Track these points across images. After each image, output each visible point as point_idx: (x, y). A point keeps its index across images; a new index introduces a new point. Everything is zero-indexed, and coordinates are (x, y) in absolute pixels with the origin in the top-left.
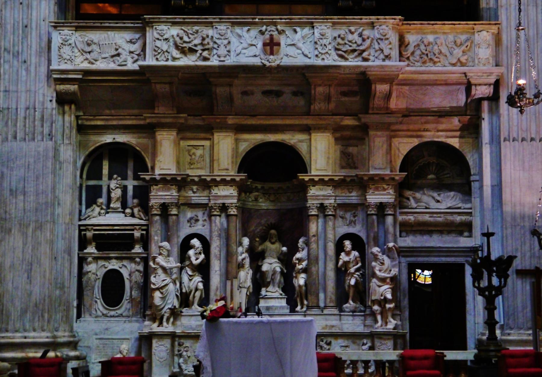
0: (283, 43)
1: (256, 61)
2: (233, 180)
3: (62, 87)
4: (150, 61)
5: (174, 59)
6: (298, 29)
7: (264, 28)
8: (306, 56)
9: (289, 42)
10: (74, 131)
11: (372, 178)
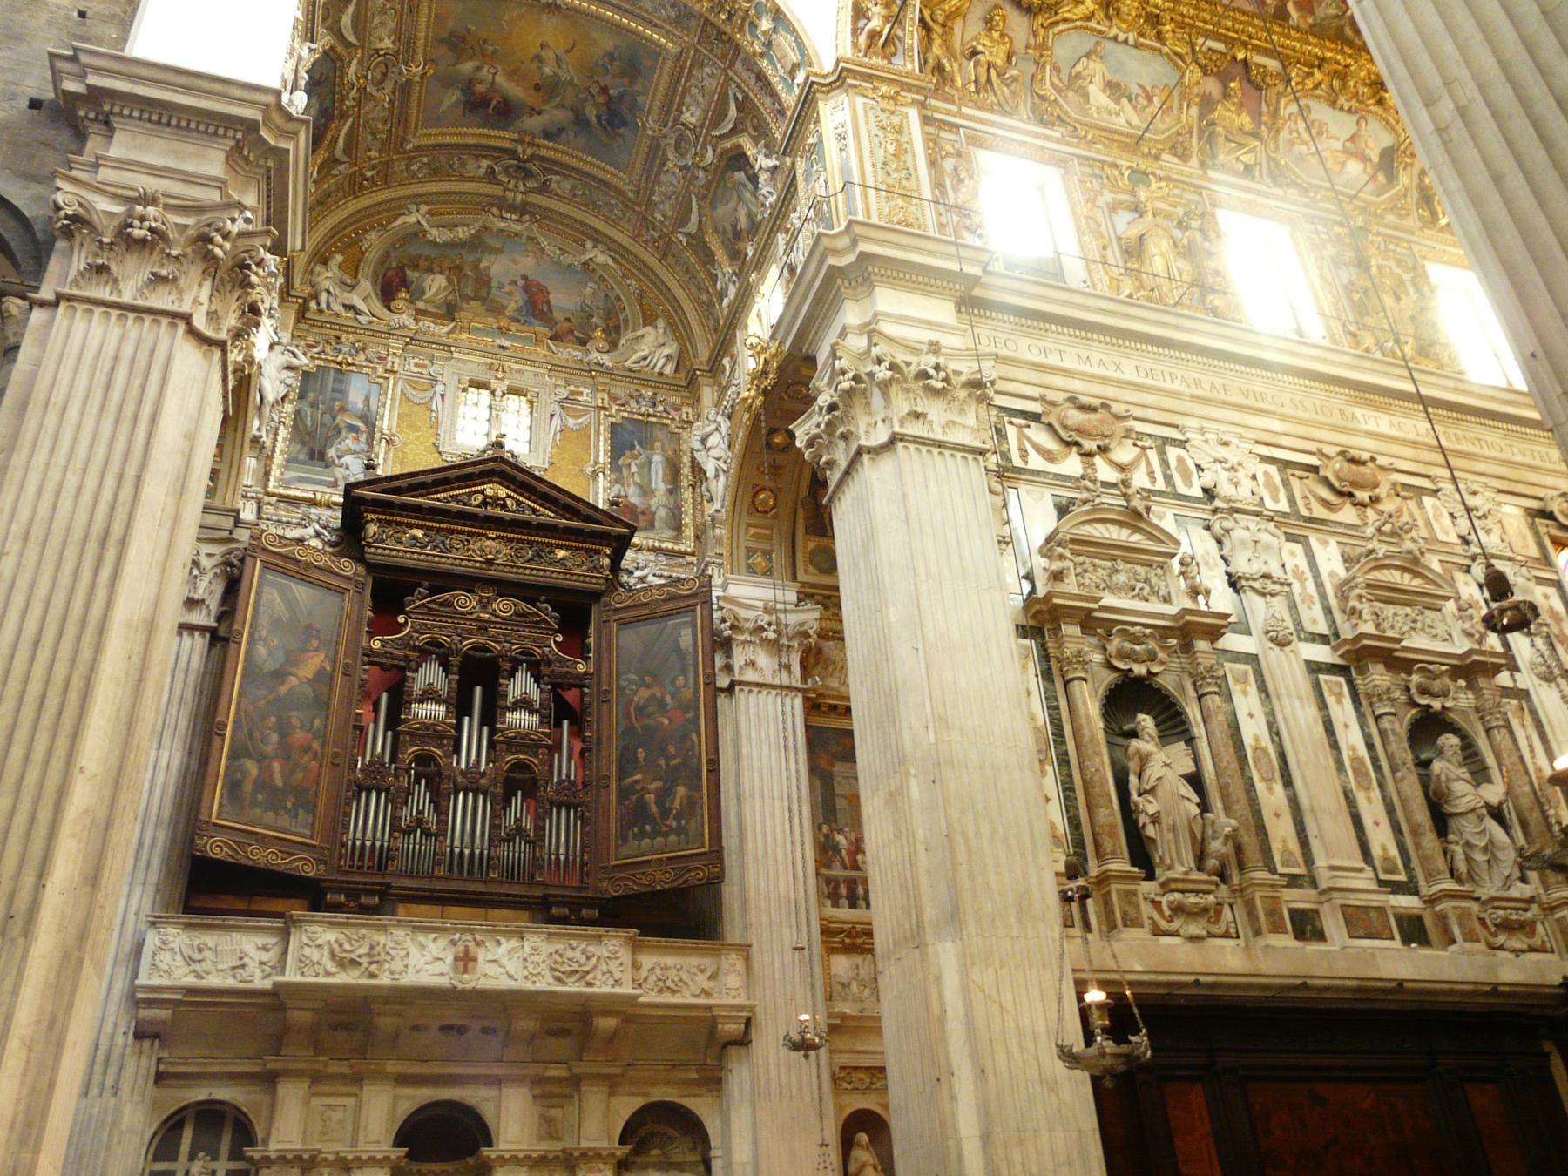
0: (481, 958)
1: (444, 982)
2: (386, 1158)
3: (144, 1013)
4: (291, 976)
5: (328, 974)
6: (503, 940)
7: (457, 936)
8: (511, 977)
9: (490, 957)
10: (151, 1081)
11: (585, 1156)
